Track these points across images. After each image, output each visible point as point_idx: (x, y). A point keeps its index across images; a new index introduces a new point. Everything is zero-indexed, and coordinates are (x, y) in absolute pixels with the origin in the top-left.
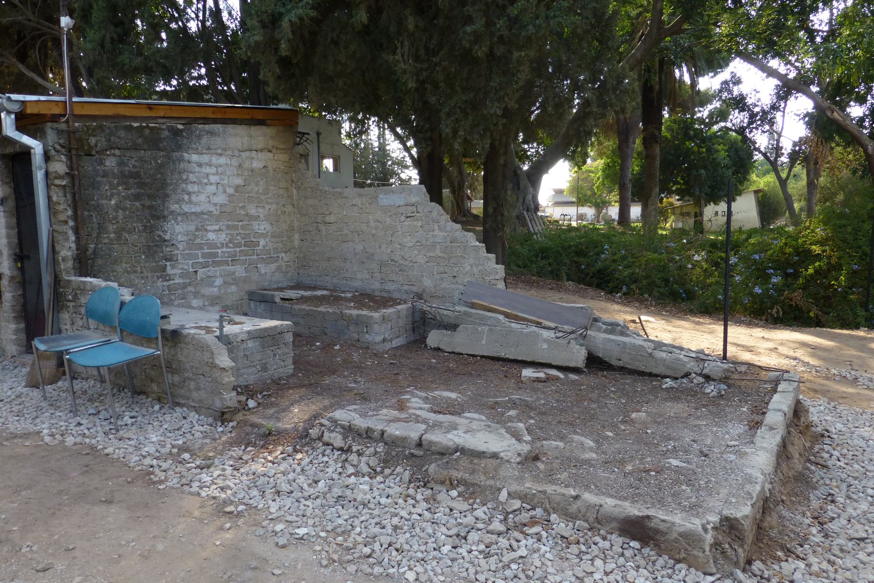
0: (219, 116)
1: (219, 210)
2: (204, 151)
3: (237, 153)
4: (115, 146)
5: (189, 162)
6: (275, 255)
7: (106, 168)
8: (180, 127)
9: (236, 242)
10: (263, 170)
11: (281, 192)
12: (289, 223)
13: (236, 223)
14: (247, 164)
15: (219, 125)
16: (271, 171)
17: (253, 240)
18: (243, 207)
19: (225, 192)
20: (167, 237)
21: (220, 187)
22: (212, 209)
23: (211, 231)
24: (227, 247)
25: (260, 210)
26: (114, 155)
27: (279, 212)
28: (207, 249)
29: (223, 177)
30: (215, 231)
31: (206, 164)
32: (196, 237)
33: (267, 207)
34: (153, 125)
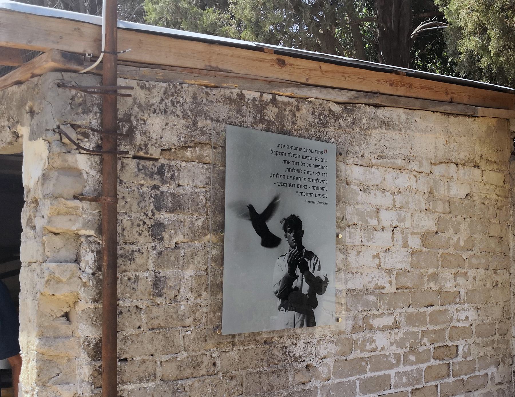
0: (401, 91)
1: (394, 283)
2: (374, 161)
3: (426, 168)
4: (203, 139)
5: (347, 183)
6: (482, 372)
7: (180, 190)
8: (337, 109)
9: (421, 349)
10: (466, 202)
11: (493, 244)
12: (502, 303)
13: (423, 309)
14: (441, 192)
15: (401, 110)
16: (477, 202)
17: (449, 343)
18: (434, 277)
19: (405, 245)
20: (298, 351)
21: (398, 236)
22: (383, 281)
23: (379, 329)
24: (406, 362)
25: (461, 281)
26: (200, 160)
27: (489, 285)
28: (372, 370)
29: (403, 213)
30: (385, 328)
31: (377, 187)
32: (352, 345)
33: (472, 273)
34: (286, 99)
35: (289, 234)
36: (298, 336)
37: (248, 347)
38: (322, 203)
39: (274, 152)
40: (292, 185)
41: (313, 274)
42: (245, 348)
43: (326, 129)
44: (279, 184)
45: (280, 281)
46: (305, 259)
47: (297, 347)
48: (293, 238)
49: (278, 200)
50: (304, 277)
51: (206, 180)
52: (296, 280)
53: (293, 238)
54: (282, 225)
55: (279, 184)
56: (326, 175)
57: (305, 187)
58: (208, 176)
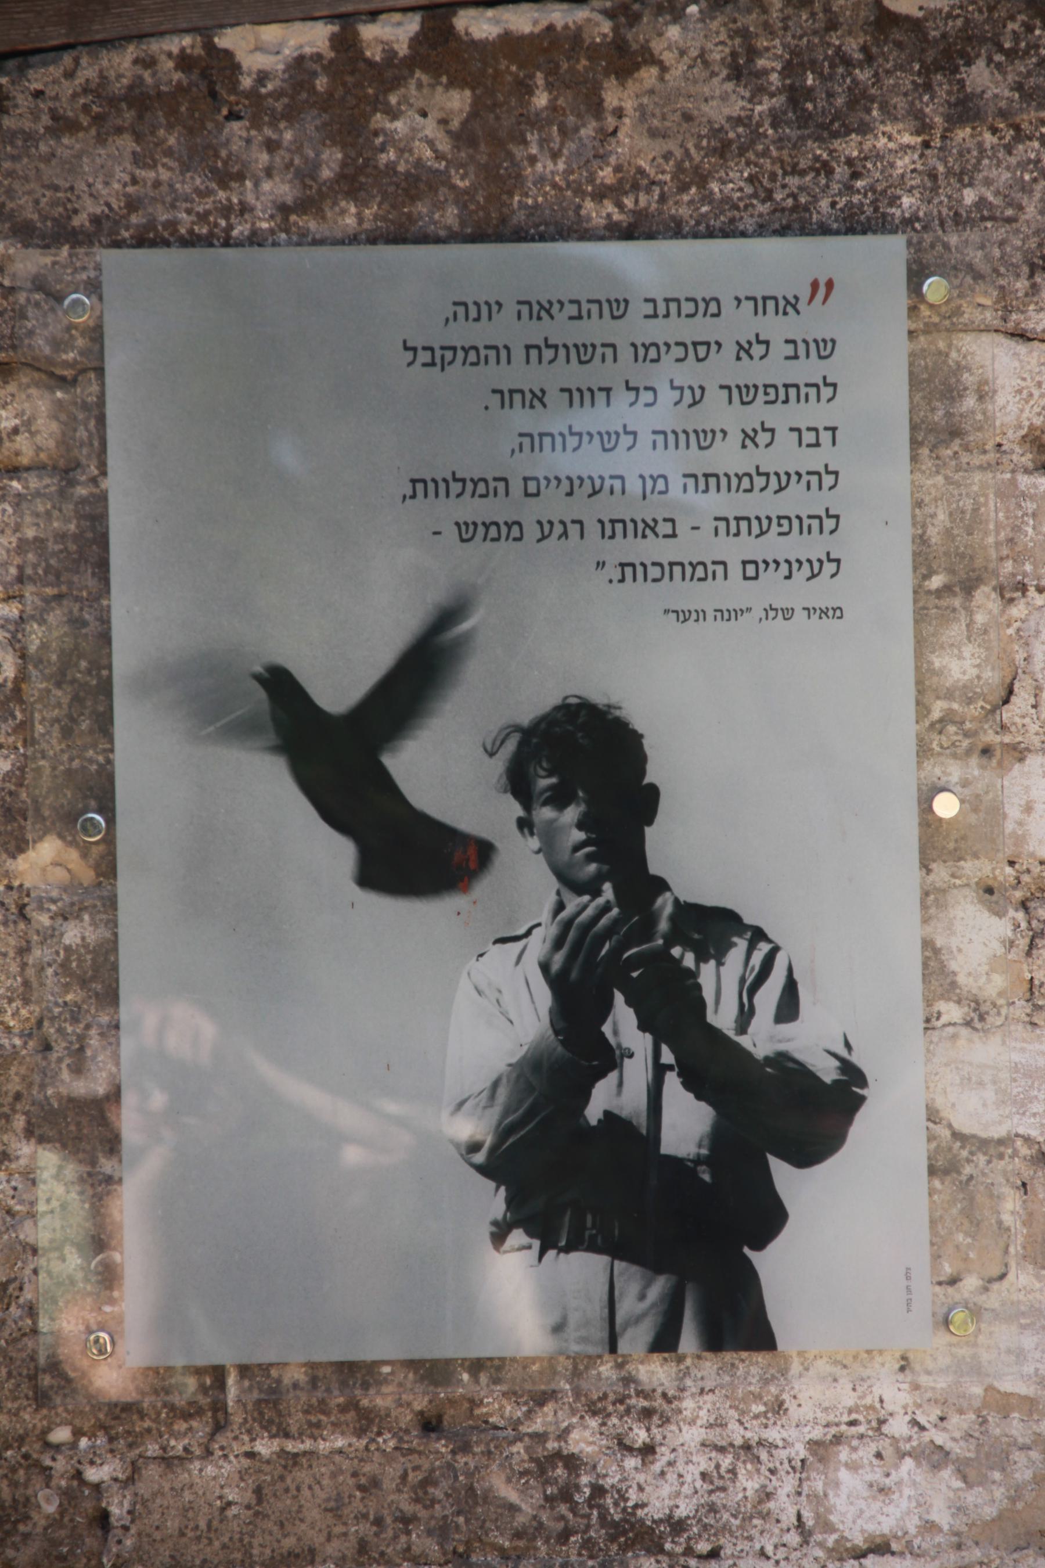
35: (546, 813)
36: (658, 1403)
37: (307, 1445)
38: (800, 615)
39: (424, 357)
40: (558, 529)
41: (744, 1041)
42: (291, 1446)
43: (850, 147)
44: (466, 531)
45: (496, 1085)
46: (676, 951)
47: (657, 1467)
48: (579, 836)
49: (465, 626)
50: (667, 1057)
51: (17, 561)
52: (613, 1076)
53: (579, 836)
54: (498, 765)
55: (466, 531)
56: (825, 437)
57: (664, 528)
58: (30, 533)
